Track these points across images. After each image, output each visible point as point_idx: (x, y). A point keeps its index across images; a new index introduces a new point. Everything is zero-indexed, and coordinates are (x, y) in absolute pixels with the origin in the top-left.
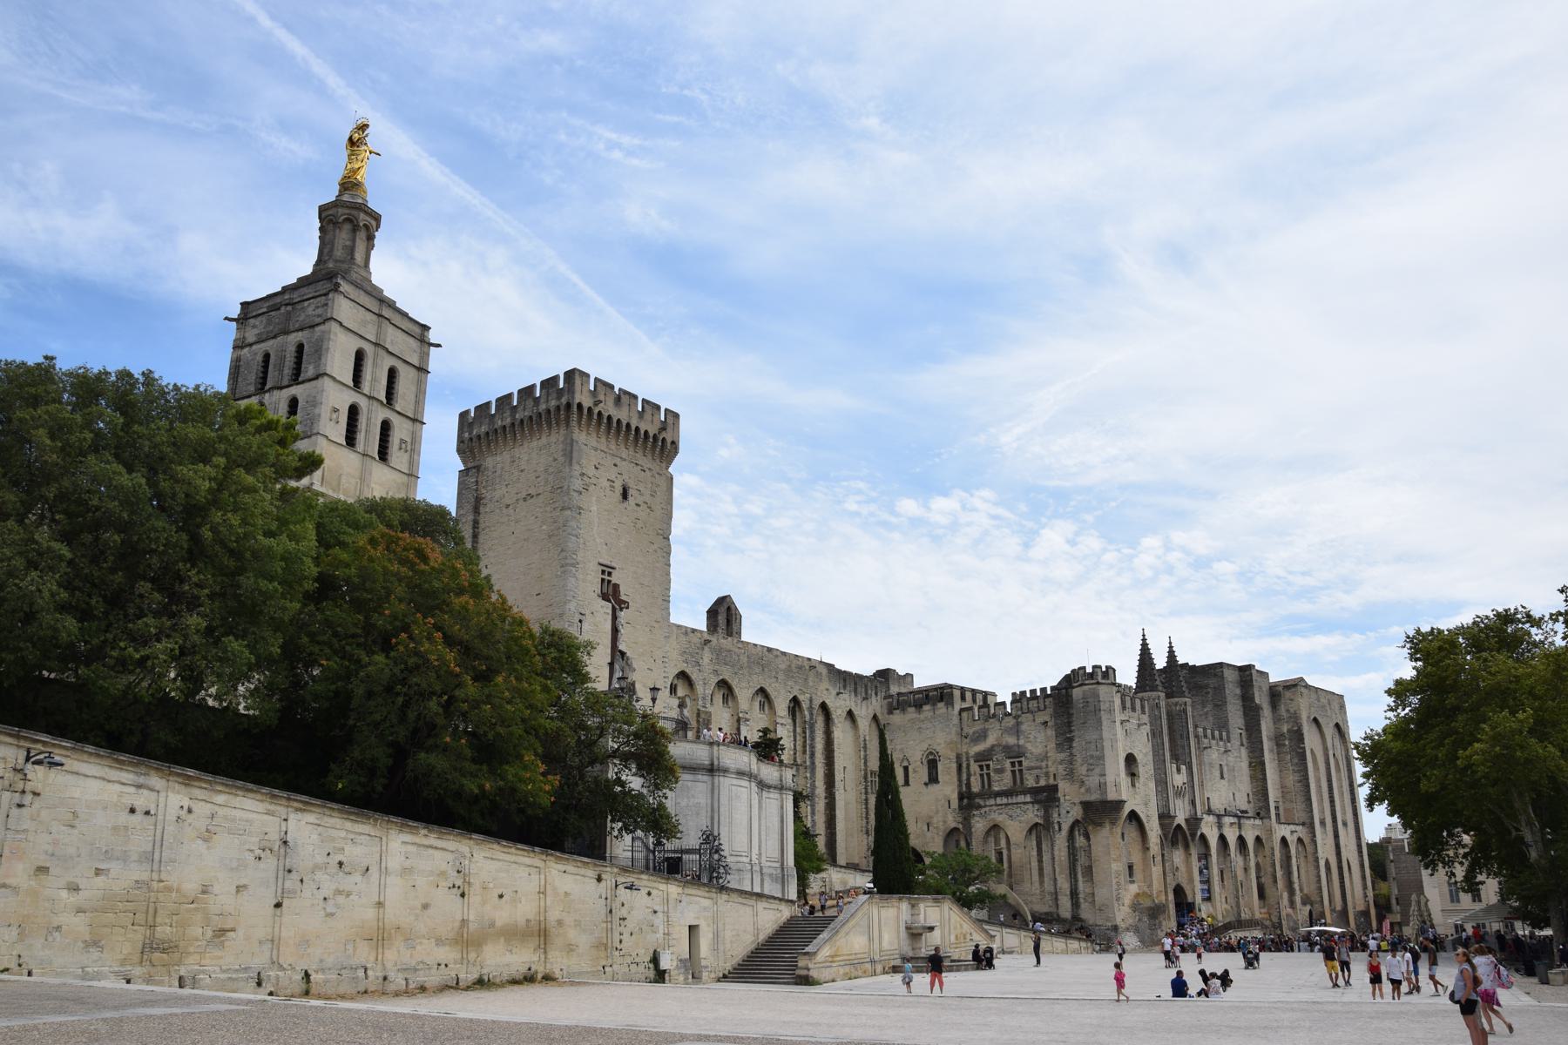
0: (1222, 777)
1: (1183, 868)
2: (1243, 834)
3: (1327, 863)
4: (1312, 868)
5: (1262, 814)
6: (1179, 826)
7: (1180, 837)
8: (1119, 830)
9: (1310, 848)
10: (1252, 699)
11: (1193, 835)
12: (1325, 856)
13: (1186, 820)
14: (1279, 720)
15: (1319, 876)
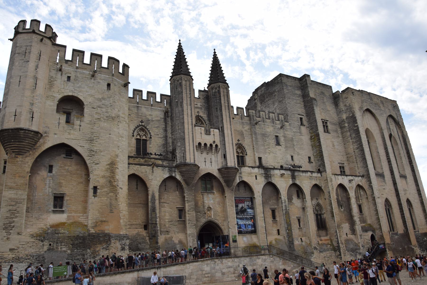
0: (278, 144)
1: (218, 208)
2: (298, 182)
3: (387, 201)
4: (371, 205)
5: (321, 169)
6: (209, 176)
7: (215, 184)
8: (29, 161)
9: (369, 192)
10: (308, 95)
11: (229, 182)
12: (385, 196)
13: (219, 170)
14: (340, 112)
15: (376, 210)
